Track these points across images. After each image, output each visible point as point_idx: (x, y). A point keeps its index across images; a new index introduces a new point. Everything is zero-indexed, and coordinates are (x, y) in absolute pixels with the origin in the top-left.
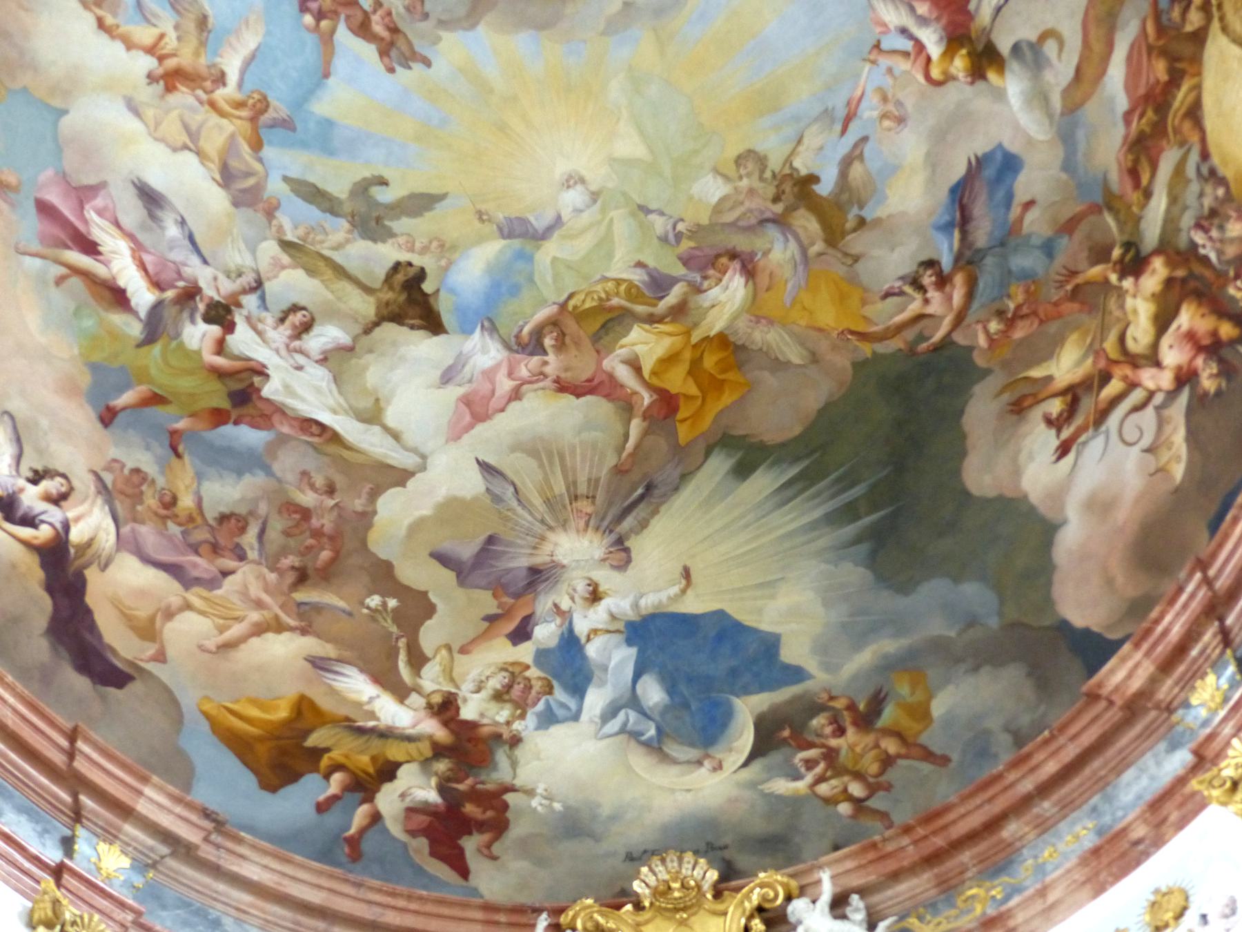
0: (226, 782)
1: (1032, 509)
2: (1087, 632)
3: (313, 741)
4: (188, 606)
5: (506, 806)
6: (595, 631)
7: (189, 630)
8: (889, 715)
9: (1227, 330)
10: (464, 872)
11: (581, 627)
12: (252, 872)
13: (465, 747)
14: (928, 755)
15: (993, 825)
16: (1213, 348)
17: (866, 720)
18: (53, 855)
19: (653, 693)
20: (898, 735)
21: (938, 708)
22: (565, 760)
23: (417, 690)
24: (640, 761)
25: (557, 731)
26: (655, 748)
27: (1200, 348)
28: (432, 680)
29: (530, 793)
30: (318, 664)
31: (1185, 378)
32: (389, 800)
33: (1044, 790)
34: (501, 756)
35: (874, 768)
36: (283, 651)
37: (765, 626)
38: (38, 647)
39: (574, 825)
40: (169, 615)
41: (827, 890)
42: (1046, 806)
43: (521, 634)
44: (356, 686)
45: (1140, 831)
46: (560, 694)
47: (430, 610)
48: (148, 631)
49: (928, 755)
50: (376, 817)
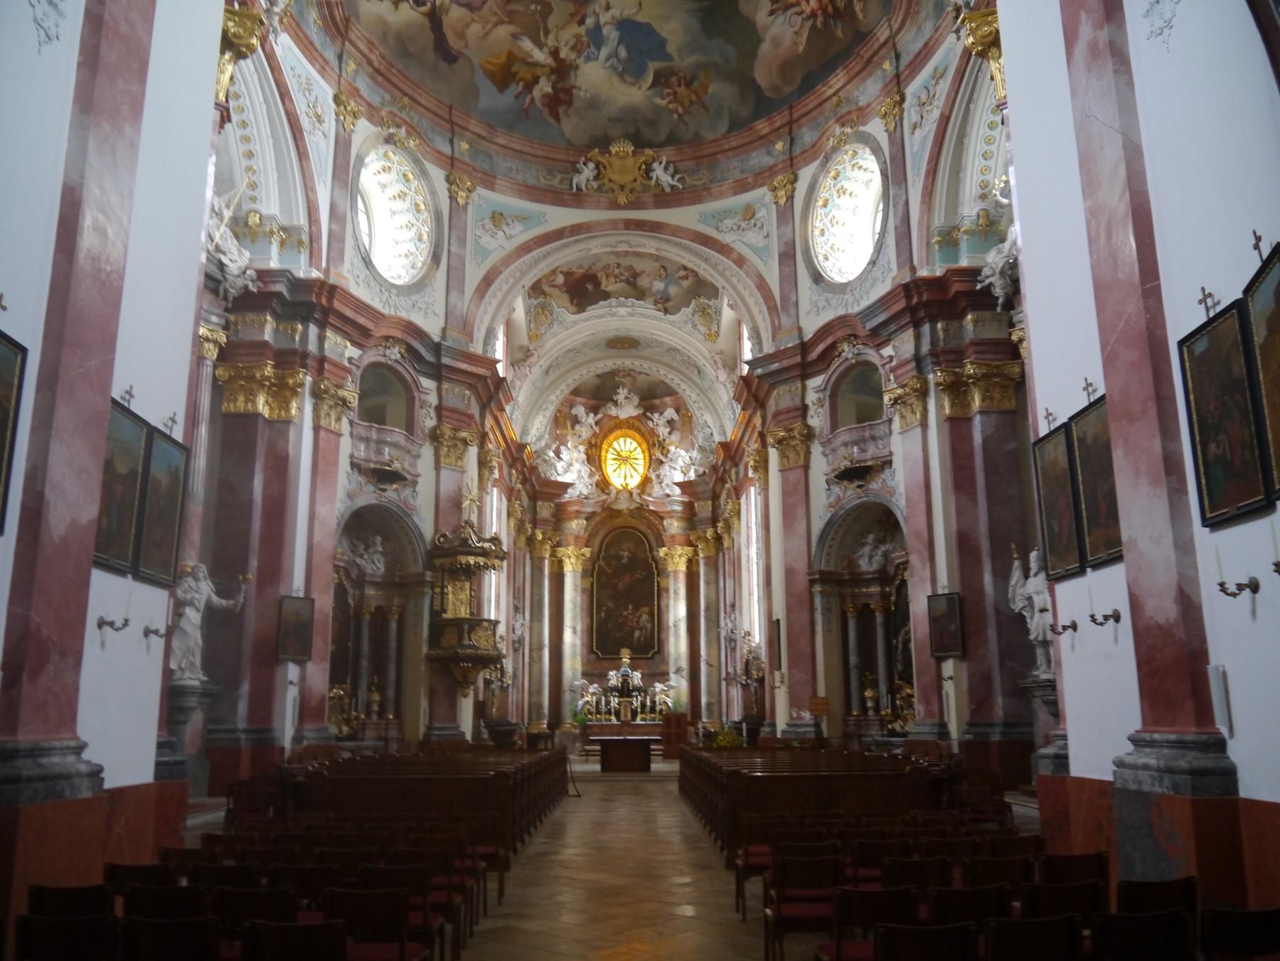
0: (490, 97)
1: (755, 30)
2: (759, 87)
3: (514, 69)
4: (473, 20)
5: (571, 95)
6: (606, 23)
7: (475, 29)
8: (696, 84)
9: (830, 8)
10: (558, 120)
11: (602, 20)
12: (501, 141)
13: (562, 70)
14: (704, 106)
15: (716, 154)
16: (825, 11)
17: (689, 84)
18: (447, 150)
19: (623, 53)
20: (696, 94)
21: (711, 89)
22: (593, 76)
23: (546, 45)
24: (616, 80)
25: (592, 64)
26: (621, 75)
27: (821, 8)
28: (551, 41)
29: (580, 89)
30: (515, 36)
31: (813, 15)
32: (537, 93)
33: (731, 149)
34: (572, 74)
35: (687, 104)
36: (503, 31)
37: (663, 34)
38: (431, 56)
39: (594, 104)
40: (467, 26)
41: (664, 160)
42: (730, 154)
43: (581, 22)
44: (527, 44)
45: (750, 180)
46: (593, 49)
47: (551, 10)
48: (461, 36)
49: (704, 106)
50: (533, 99)
